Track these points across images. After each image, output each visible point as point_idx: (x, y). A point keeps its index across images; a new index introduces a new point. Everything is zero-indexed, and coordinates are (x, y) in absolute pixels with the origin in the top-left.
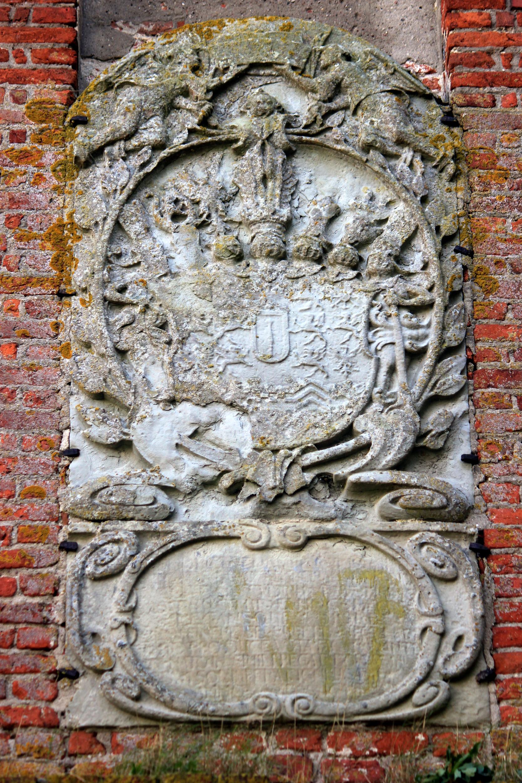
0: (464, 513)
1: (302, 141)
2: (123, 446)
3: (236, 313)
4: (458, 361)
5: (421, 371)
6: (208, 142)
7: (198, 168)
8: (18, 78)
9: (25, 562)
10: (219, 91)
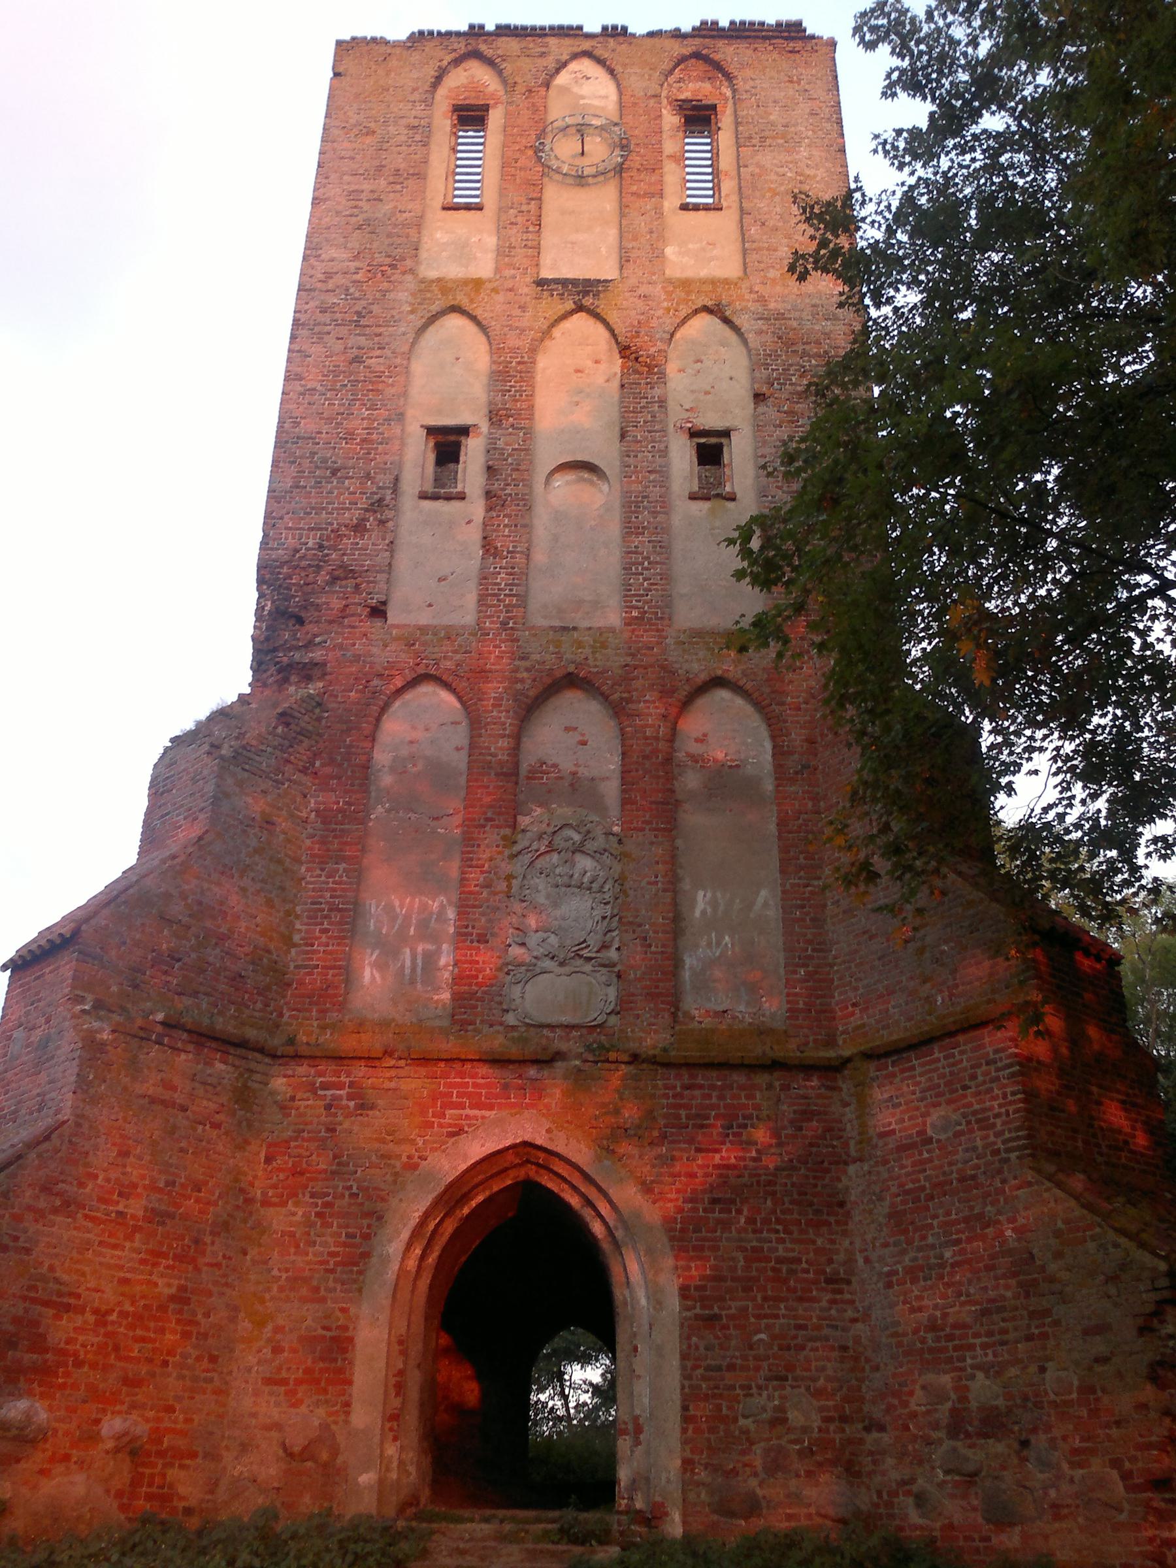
0: (614, 965)
1: (579, 849)
2: (523, 944)
3: (556, 905)
6: (551, 849)
7: (547, 857)
8: (498, 827)
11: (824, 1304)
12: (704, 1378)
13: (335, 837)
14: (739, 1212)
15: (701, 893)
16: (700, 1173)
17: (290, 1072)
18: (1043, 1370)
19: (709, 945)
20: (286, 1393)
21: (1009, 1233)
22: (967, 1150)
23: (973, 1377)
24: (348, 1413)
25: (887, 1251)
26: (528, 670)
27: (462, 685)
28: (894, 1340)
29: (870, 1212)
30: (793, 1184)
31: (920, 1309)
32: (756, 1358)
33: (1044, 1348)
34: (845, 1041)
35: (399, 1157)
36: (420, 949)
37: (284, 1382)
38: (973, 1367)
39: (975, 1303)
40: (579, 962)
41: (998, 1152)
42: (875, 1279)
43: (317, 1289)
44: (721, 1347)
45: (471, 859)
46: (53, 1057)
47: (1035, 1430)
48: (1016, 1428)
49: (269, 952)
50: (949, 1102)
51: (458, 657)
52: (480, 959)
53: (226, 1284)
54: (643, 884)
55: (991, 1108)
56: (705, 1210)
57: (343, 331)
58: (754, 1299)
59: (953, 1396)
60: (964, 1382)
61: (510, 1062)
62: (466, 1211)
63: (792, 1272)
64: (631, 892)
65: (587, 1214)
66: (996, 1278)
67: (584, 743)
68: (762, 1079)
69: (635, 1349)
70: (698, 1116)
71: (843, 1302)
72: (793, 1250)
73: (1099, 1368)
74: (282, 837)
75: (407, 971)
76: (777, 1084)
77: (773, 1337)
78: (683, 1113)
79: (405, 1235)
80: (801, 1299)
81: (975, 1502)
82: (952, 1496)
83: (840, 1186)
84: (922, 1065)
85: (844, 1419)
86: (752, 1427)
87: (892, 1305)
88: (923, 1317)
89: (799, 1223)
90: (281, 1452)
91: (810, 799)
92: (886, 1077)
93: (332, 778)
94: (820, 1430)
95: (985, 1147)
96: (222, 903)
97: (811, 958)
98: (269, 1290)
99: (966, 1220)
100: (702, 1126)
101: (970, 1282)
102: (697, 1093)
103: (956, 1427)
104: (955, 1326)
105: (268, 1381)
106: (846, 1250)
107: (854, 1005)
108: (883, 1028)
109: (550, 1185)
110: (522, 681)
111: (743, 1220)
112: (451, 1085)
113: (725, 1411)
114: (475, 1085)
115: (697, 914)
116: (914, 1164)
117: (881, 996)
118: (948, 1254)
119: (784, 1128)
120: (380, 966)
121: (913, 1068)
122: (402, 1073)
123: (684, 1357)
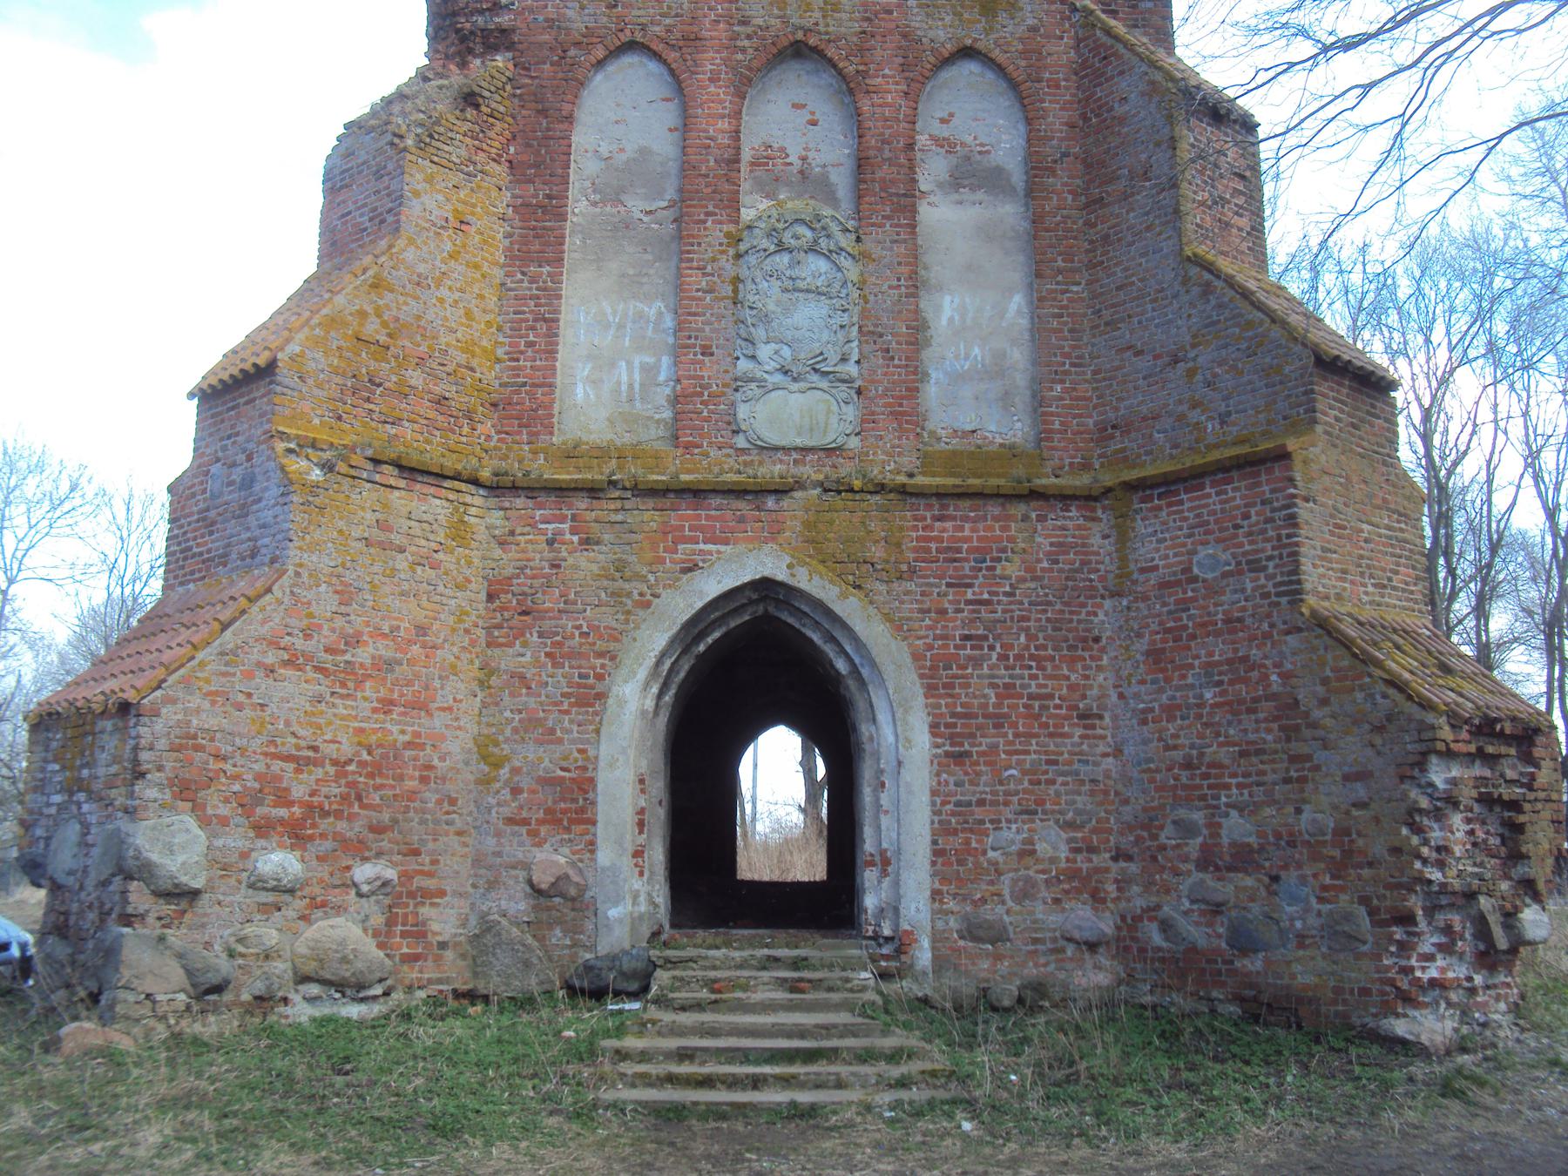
2: (753, 357)
3: (787, 311)
4: (856, 328)
8: (721, 223)
9: (723, 394)
11: (1076, 739)
12: (953, 814)
13: (536, 236)
14: (991, 648)
15: (948, 299)
16: (951, 608)
17: (507, 505)
18: (1299, 811)
19: (957, 357)
20: (529, 833)
21: (1274, 678)
22: (1236, 591)
23: (1227, 815)
24: (592, 852)
25: (1143, 688)
26: (749, 37)
27: (672, 56)
28: (1145, 776)
29: (1127, 648)
30: (1048, 620)
31: (1175, 747)
32: (1006, 793)
33: (1302, 791)
34: (1102, 465)
35: (629, 595)
36: (637, 363)
37: (525, 822)
38: (1228, 805)
39: (1235, 745)
40: (815, 377)
41: (1266, 596)
42: (1129, 715)
43: (552, 731)
44: (972, 783)
45: (691, 260)
46: (260, 500)
47: (1285, 867)
48: (1267, 864)
49: (472, 370)
50: (1218, 541)
51: (668, 21)
52: (706, 374)
53: (460, 728)
54: (885, 287)
55: (1263, 550)
56: (956, 647)
58: (1005, 735)
59: (1205, 831)
60: (1217, 819)
61: (746, 492)
62: (702, 648)
63: (1042, 707)
64: (872, 298)
65: (829, 649)
66: (1257, 721)
67: (814, 123)
68: (1018, 509)
69: (883, 785)
70: (949, 549)
71: (1095, 737)
72: (1046, 686)
73: (1355, 813)
74: (478, 238)
75: (624, 388)
76: (1034, 515)
77: (1024, 773)
78: (933, 546)
80: (1051, 735)
81: (1221, 930)
82: (1197, 924)
83: (1096, 620)
84: (1190, 500)
85: (1092, 850)
86: (1001, 860)
87: (1145, 742)
88: (1178, 755)
89: (1052, 659)
90: (528, 889)
91: (1070, 192)
92: (1150, 510)
93: (530, 167)
94: (1068, 860)
95: (1254, 590)
96: (419, 318)
97: (1066, 373)
98: (502, 732)
99: (1230, 662)
100: (955, 560)
101: (1230, 723)
102: (949, 525)
103: (1206, 861)
104: (1210, 766)
105: (510, 821)
106: (1100, 686)
107: (1114, 427)
108: (1148, 453)
109: (791, 620)
110: (743, 50)
111: (995, 656)
112: (681, 518)
113: (974, 845)
114: (708, 518)
115: (944, 322)
116: (1177, 602)
117: (1144, 419)
118: (1208, 695)
119: (1039, 561)
120: (595, 383)
121: (1181, 502)
122: (628, 505)
123: (934, 793)
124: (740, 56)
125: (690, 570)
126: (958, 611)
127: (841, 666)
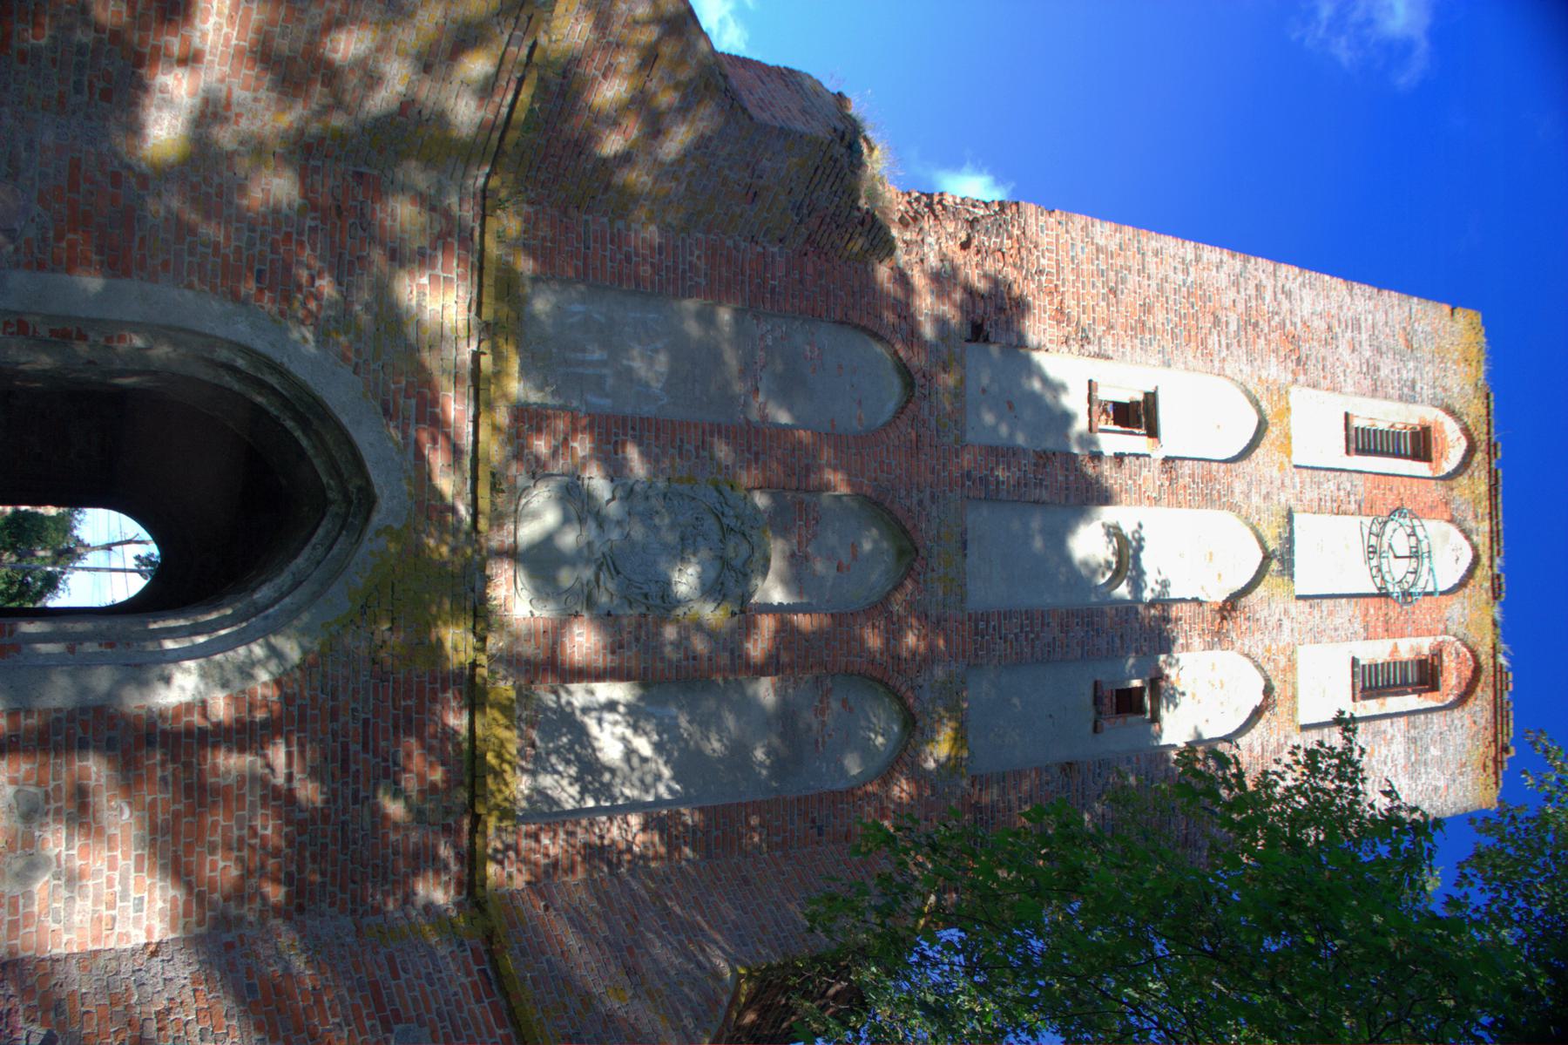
5: (640, 598)
6: (726, 531)
7: (716, 527)
10: (744, 534)
24: (28, 265)
26: (920, 502)
30: (324, 846)
36: (605, 371)
51: (933, 423)
57: (1241, 307)
62: (289, 424)
65: (285, 579)
70: (409, 720)
74: (738, 211)
79: (260, 345)
83: (324, 906)
100: (396, 727)
105: (75, 165)
109: (321, 531)
121: (479, 1000)
124: (903, 493)
125: (386, 412)
126: (334, 734)
127: (263, 593)
